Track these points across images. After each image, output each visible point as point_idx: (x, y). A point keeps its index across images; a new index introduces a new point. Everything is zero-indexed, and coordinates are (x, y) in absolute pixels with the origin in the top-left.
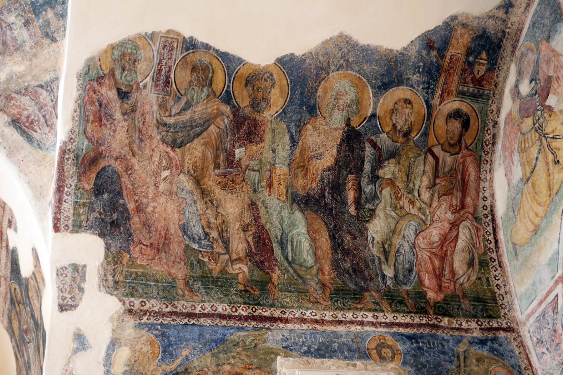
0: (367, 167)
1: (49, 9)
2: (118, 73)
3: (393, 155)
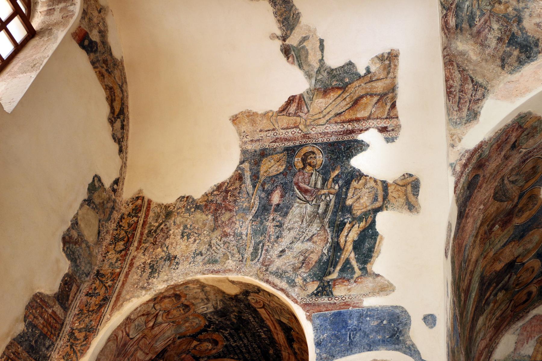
0: (500, 285)
1: (518, 50)
2: (525, 133)
3: (506, 290)
